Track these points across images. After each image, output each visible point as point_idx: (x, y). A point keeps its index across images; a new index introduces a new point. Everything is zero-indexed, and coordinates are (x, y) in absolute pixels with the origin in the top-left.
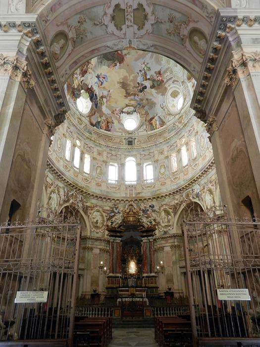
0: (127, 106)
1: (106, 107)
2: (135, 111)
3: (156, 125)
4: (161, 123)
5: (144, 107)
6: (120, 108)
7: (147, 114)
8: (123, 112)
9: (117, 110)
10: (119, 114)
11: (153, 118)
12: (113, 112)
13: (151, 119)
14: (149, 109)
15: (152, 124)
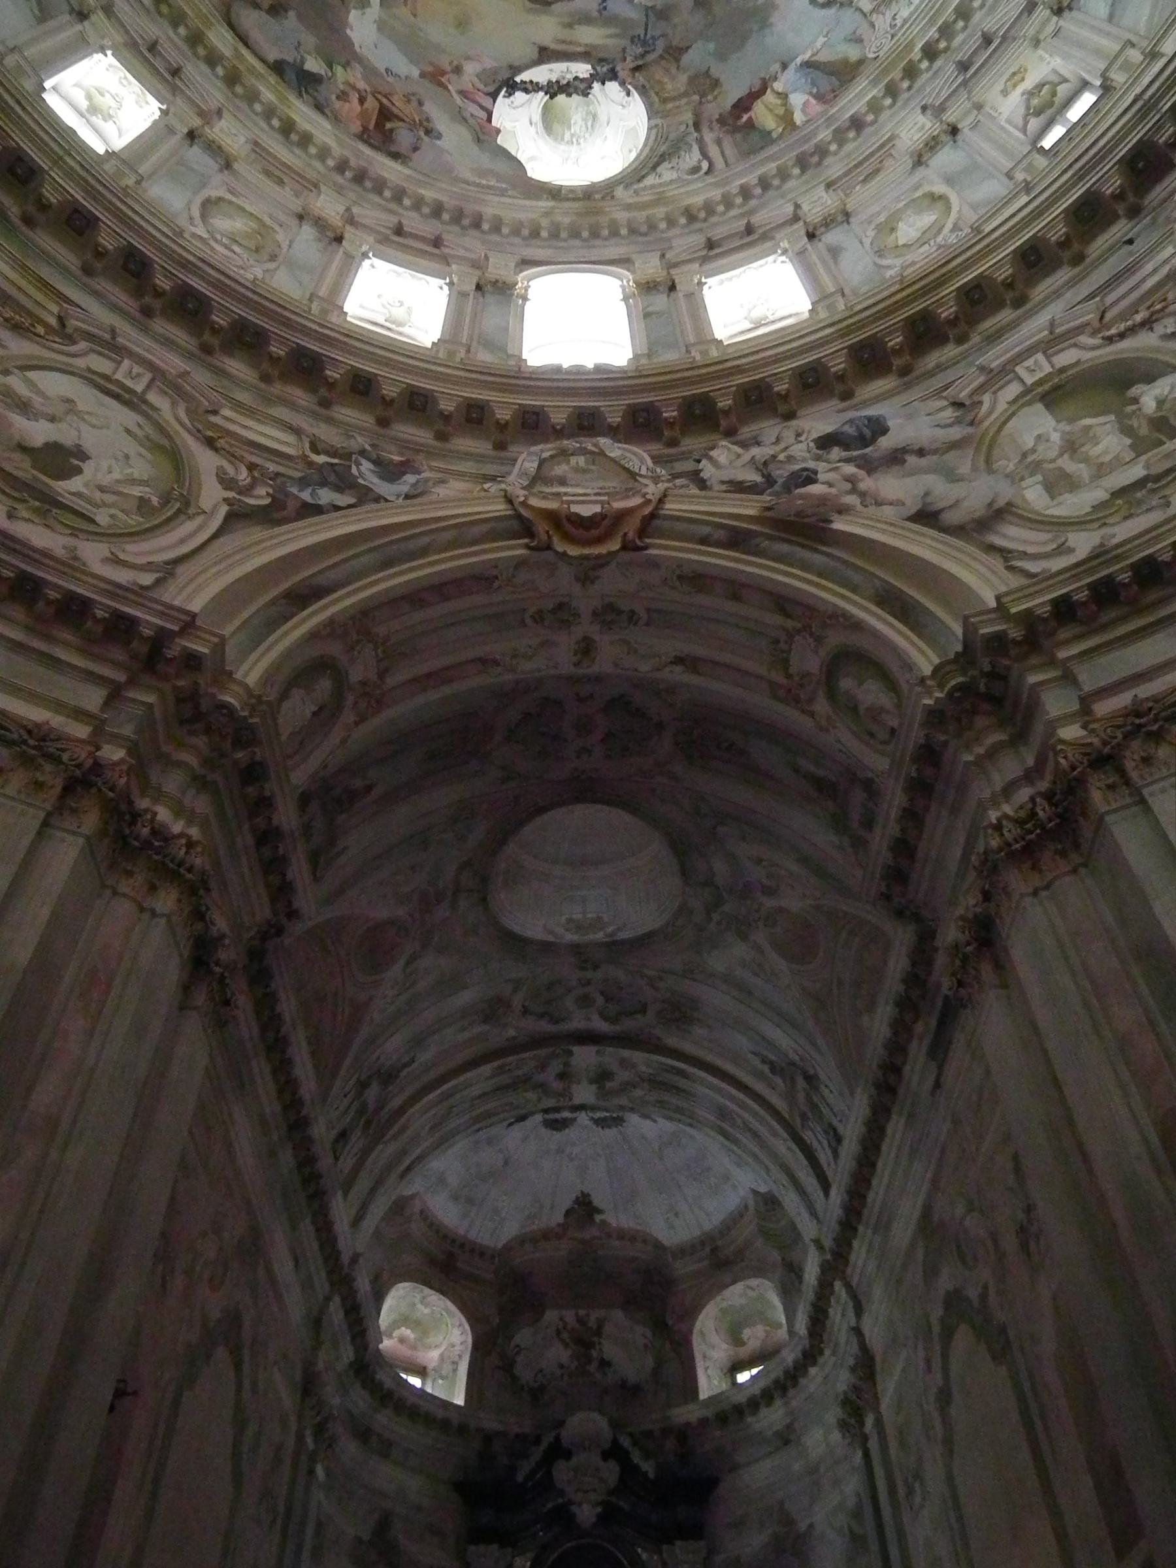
0: (545, 55)
1: (382, 26)
2: (613, 75)
3: (787, 119)
4: (825, 83)
5: (675, 53)
6: (489, 63)
7: (705, 83)
8: (512, 87)
9: (470, 69)
10: (486, 102)
11: (762, 92)
12: (436, 77)
13: (744, 105)
14: (722, 56)
15: (750, 125)
